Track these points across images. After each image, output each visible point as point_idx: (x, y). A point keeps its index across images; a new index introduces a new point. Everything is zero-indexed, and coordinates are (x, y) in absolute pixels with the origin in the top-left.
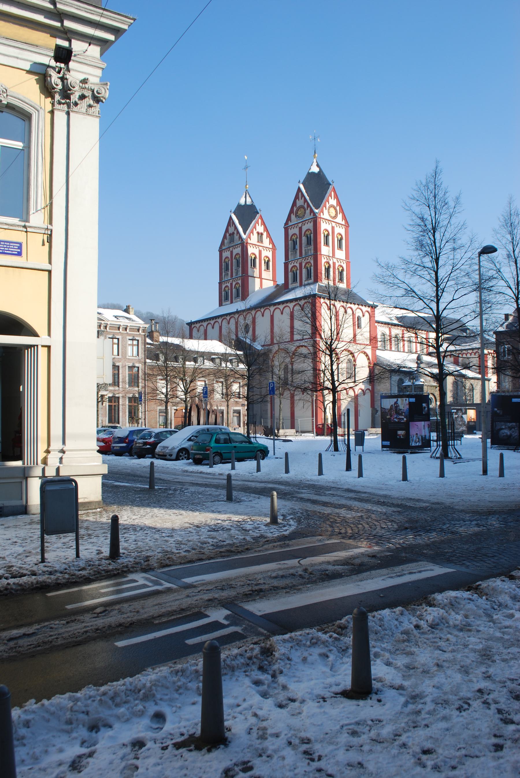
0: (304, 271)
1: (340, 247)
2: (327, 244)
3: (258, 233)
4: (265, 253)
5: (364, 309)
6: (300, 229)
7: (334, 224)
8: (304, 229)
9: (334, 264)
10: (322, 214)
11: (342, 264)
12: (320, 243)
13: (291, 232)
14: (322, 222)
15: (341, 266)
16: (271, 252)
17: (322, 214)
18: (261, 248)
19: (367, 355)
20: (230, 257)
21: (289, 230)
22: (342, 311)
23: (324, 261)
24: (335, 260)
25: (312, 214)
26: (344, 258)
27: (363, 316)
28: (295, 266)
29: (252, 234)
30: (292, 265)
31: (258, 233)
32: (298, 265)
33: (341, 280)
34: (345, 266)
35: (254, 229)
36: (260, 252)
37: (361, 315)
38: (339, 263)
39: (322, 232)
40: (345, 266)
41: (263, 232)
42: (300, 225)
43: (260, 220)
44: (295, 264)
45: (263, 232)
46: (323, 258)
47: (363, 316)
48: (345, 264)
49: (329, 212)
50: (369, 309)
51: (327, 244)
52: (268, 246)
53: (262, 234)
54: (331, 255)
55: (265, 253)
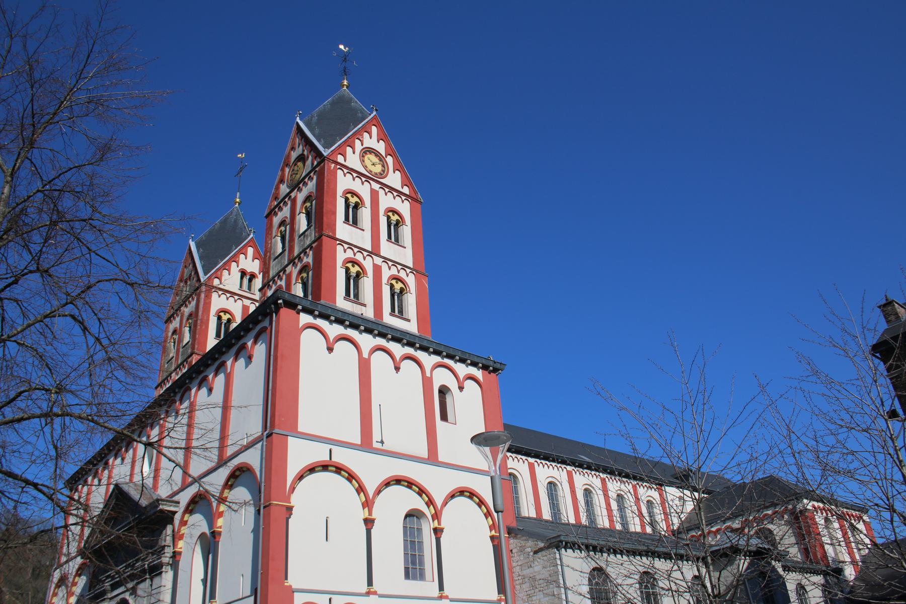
2: (352, 219)
3: (243, 273)
5: (462, 370)
7: (376, 186)
9: (377, 270)
12: (334, 213)
14: (339, 172)
19: (481, 503)
22: (380, 362)
23: (341, 255)
24: (378, 261)
27: (461, 388)
29: (225, 272)
31: (243, 273)
33: (398, 310)
35: (234, 264)
37: (452, 384)
38: (394, 271)
39: (340, 192)
41: (257, 271)
45: (258, 274)
46: (339, 249)
47: (461, 388)
48: (412, 276)
49: (362, 161)
50: (478, 373)
53: (253, 276)
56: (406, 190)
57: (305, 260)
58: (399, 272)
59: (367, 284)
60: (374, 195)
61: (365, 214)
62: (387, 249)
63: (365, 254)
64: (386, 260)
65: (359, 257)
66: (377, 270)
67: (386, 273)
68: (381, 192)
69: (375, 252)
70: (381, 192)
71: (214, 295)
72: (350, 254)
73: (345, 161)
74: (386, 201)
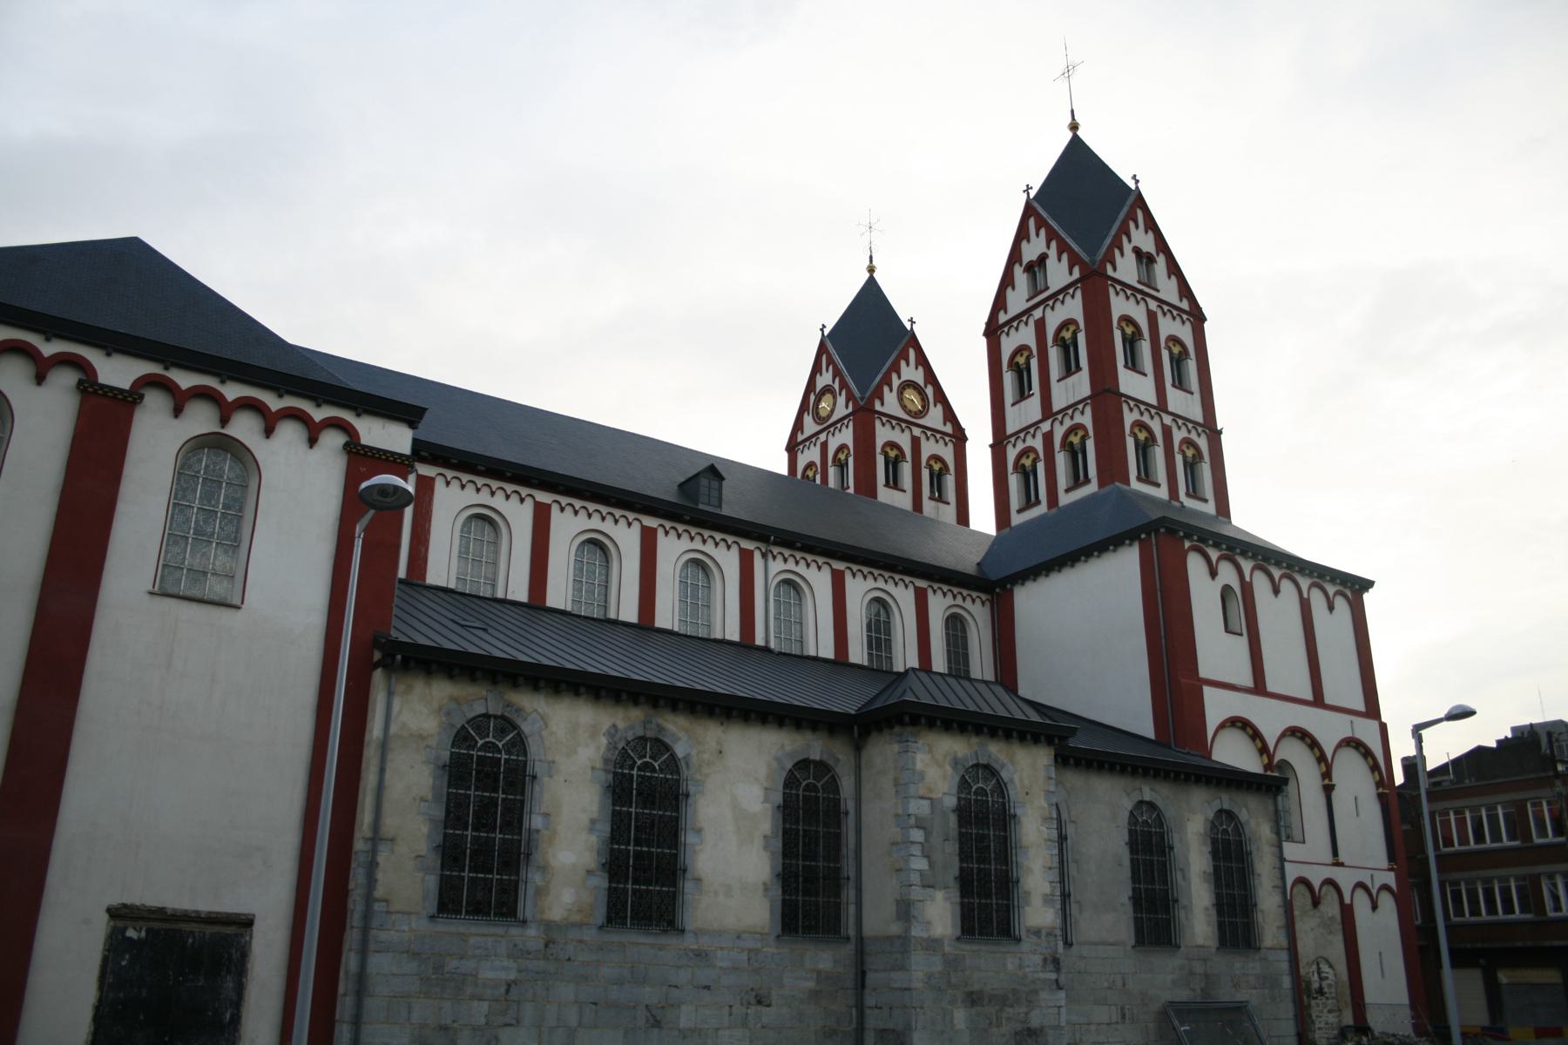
0: (1061, 460)
1: (1180, 383)
2: (1133, 364)
4: (929, 448)
6: (1040, 325)
8: (1053, 321)
9: (1167, 432)
10: (1109, 267)
11: (1193, 436)
13: (1008, 345)
15: (1188, 442)
16: (951, 446)
17: (1109, 267)
18: (917, 432)
20: (818, 462)
21: (1003, 338)
23: (1129, 418)
24: (1168, 420)
25: (1076, 271)
26: (1201, 420)
28: (1031, 449)
30: (1020, 446)
32: (1038, 443)
34: (1203, 443)
36: (916, 442)
40: (1203, 443)
42: (1037, 314)
43: (912, 353)
44: (1030, 442)
48: (1203, 436)
51: (1133, 364)
52: (940, 427)
54: (1153, 400)
55: (929, 448)
56: (1185, 305)
57: (1078, 419)
58: (1189, 432)
59: (1159, 453)
60: (1152, 317)
61: (1145, 347)
62: (1176, 400)
63: (1153, 411)
64: (1175, 416)
65: (1146, 419)
66: (1167, 432)
67: (1178, 436)
68: (1160, 314)
69: (1162, 406)
70: (1160, 314)
71: (878, 424)
72: (1135, 416)
73: (1115, 269)
74: (1167, 327)
